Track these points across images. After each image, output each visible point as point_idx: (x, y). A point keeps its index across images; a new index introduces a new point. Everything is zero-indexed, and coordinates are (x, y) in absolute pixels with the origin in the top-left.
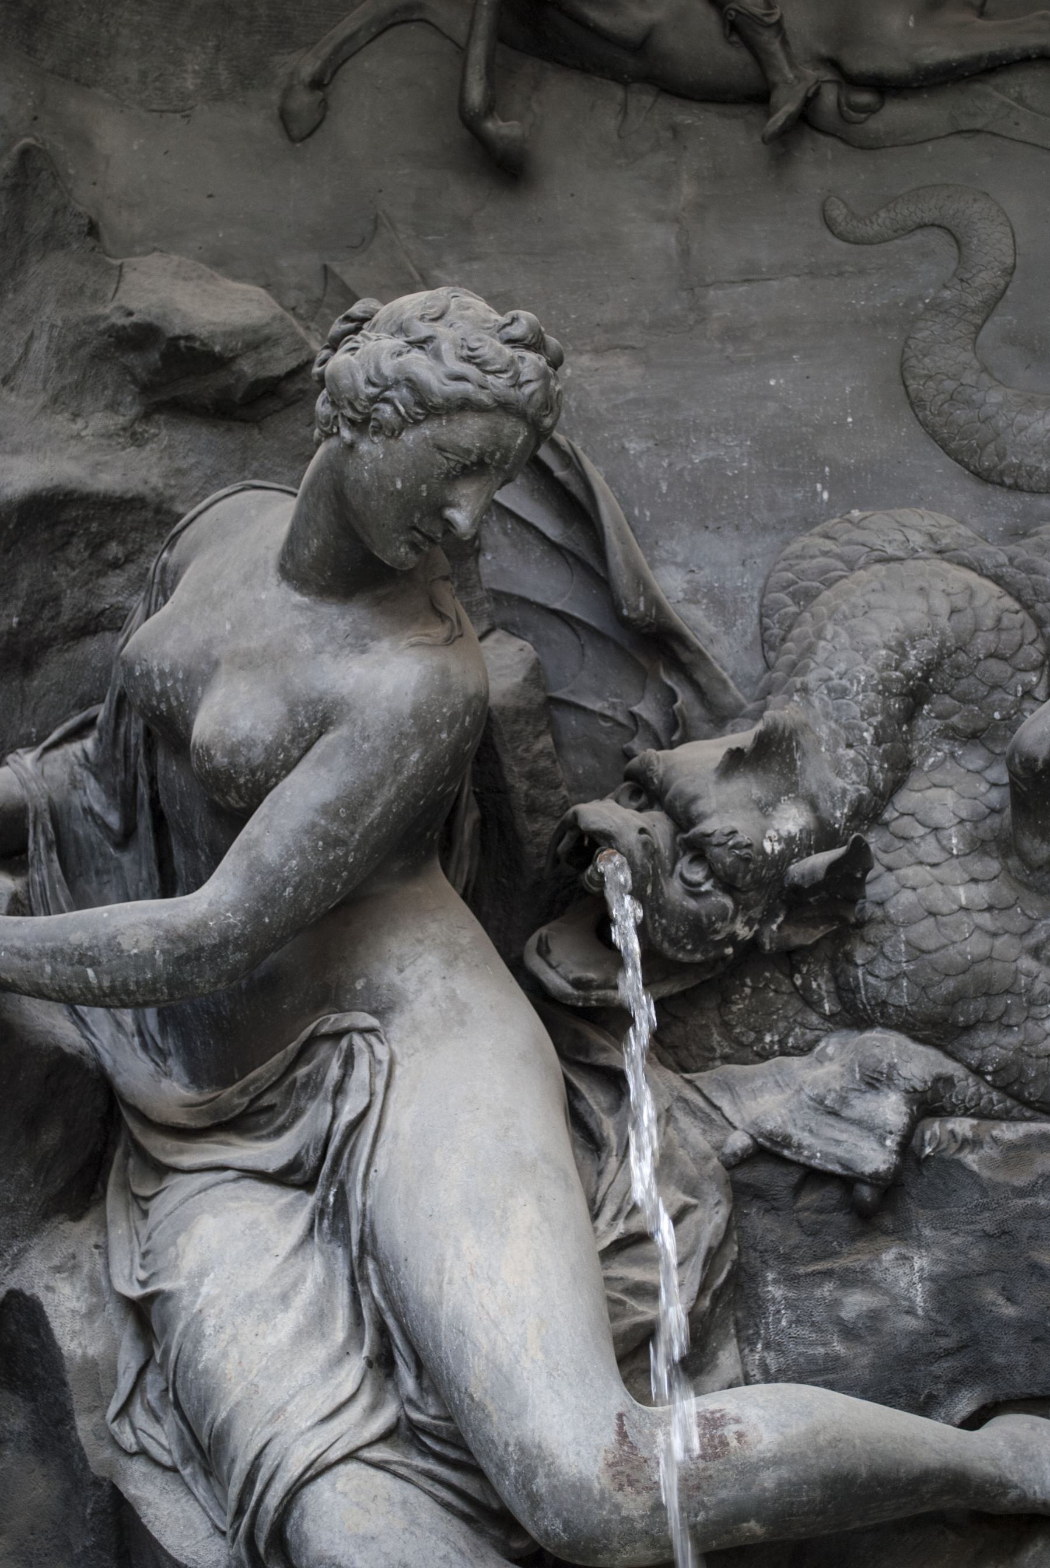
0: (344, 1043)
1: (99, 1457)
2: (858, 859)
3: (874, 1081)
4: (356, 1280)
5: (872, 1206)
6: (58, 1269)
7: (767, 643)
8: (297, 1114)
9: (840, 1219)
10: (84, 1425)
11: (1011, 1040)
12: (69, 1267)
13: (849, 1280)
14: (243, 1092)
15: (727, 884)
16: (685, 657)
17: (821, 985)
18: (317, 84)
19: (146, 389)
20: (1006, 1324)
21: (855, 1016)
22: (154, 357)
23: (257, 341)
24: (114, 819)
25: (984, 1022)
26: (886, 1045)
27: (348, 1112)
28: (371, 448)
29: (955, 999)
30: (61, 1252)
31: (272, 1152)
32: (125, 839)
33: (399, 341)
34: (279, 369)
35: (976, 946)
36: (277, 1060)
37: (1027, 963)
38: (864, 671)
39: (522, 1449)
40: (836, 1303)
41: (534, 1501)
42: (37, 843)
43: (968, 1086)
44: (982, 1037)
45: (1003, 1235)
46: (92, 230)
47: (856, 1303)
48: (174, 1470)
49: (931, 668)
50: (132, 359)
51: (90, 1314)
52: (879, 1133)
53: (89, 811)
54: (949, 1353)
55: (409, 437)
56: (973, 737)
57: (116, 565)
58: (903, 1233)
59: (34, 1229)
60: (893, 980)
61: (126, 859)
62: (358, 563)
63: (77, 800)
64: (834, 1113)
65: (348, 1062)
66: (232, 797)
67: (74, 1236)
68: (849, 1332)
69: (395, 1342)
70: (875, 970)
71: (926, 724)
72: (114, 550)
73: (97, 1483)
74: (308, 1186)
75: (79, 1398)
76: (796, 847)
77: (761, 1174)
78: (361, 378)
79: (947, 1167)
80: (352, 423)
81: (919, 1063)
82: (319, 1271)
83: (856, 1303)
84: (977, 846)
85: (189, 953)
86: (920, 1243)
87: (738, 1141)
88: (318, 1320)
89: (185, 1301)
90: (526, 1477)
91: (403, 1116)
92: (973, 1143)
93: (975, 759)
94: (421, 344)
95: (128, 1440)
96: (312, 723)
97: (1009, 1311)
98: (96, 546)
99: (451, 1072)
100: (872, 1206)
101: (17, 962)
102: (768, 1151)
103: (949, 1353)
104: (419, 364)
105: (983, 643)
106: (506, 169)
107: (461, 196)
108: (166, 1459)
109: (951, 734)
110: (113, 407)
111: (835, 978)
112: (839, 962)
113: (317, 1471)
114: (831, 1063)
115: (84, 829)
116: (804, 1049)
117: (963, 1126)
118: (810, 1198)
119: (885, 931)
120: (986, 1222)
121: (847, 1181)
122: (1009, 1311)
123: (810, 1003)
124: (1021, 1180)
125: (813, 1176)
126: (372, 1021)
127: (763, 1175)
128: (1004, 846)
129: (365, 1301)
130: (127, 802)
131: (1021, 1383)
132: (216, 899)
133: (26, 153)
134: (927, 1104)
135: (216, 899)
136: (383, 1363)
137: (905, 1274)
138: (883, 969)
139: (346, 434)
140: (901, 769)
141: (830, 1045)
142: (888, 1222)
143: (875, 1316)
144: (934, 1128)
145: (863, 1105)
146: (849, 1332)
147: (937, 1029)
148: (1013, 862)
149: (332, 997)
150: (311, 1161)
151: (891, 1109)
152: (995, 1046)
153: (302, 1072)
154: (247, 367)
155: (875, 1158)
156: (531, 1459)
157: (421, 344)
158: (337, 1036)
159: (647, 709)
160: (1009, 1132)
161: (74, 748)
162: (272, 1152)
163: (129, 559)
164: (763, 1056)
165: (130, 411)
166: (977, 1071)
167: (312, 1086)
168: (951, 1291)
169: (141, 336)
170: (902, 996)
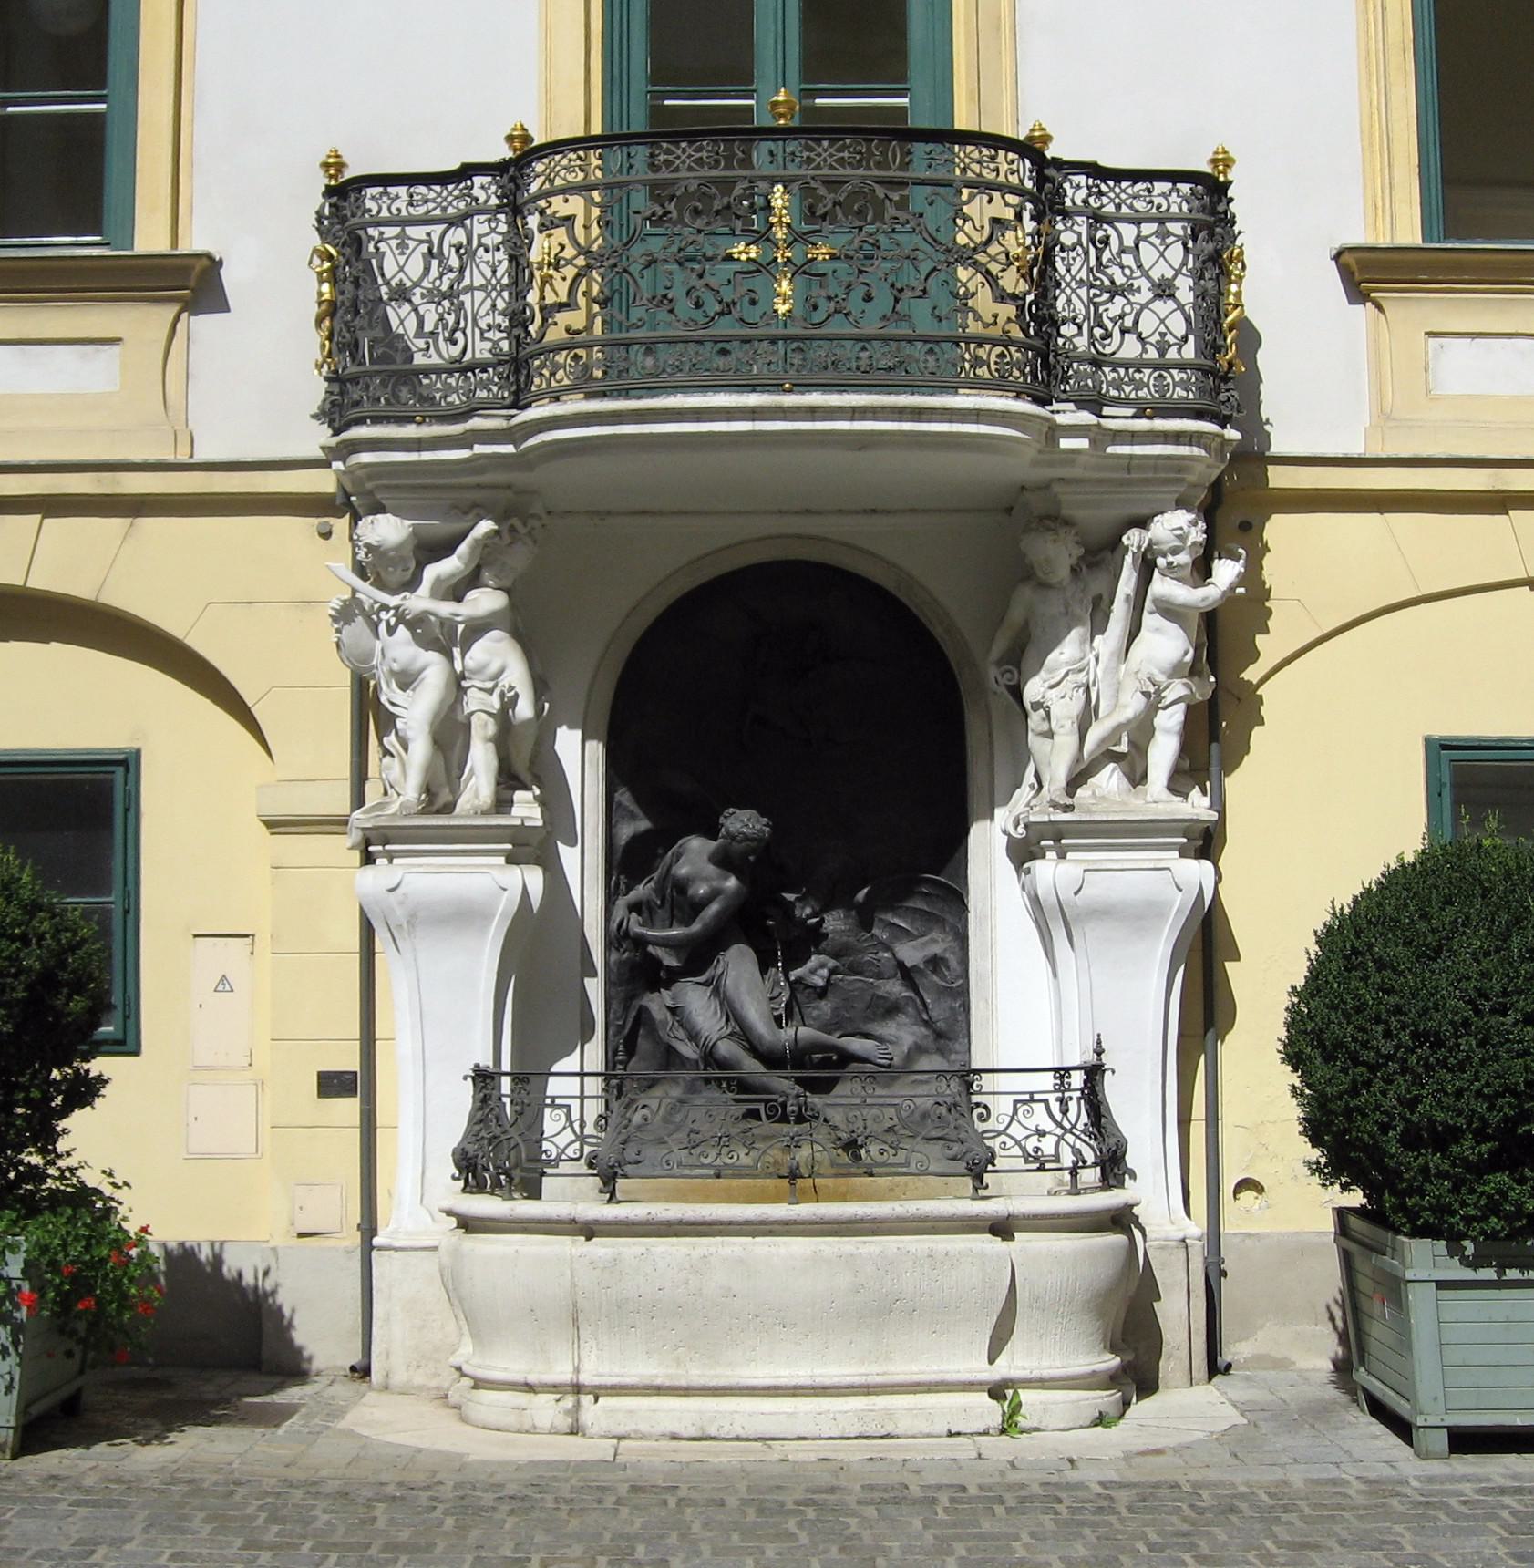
1: (666, 1039)
2: (823, 920)
3: (823, 966)
4: (721, 1004)
5: (822, 993)
26: (823, 958)
27: (719, 971)
31: (702, 979)
32: (661, 906)
62: (724, 861)
66: (697, 907)
69: (732, 1014)
76: (809, 917)
79: (835, 985)
81: (832, 963)
82: (715, 1003)
91: (732, 973)
99: (738, 965)
121: (815, 988)
125: (808, 986)
127: (796, 986)
131: (850, 1030)
132: (696, 927)
134: (833, 972)
135: (696, 927)
136: (728, 1020)
137: (826, 1007)
147: (836, 956)
151: (825, 972)
155: (821, 983)
156: (760, 1037)
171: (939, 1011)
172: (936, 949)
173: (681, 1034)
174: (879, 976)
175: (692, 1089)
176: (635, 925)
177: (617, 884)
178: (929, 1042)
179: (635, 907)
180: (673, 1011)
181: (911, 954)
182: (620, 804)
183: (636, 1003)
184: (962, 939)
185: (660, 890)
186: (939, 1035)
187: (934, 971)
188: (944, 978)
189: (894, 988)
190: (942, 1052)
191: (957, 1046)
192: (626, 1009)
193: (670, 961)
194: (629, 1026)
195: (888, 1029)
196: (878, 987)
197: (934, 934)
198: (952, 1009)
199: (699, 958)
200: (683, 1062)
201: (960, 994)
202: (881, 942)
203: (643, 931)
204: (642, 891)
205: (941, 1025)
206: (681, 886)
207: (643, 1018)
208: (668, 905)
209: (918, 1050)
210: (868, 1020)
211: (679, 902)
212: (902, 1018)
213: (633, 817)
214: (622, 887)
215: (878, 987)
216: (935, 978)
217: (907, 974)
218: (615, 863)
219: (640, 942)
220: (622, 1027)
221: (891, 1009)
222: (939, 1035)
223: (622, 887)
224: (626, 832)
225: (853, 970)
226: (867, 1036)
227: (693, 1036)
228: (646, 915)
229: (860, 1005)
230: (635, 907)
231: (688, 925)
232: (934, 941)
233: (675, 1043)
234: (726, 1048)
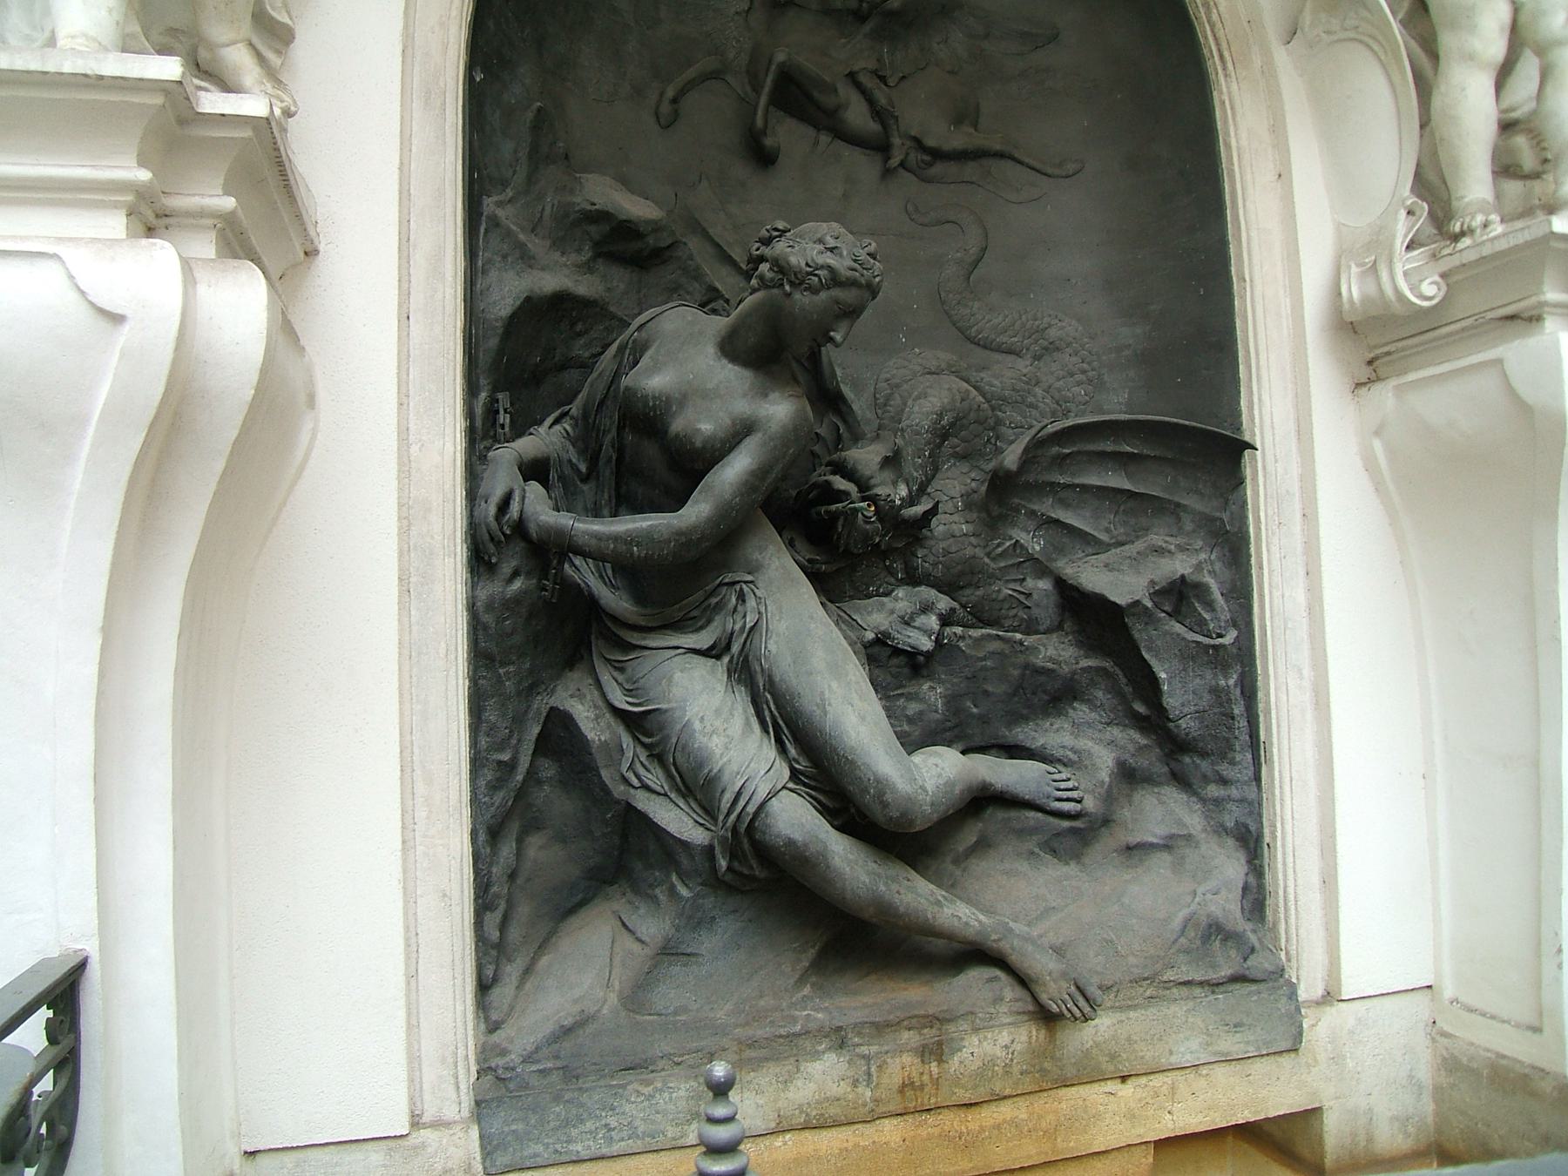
0: (738, 587)
1: (618, 790)
3: (926, 609)
6: (572, 696)
7: (880, 405)
8: (709, 622)
9: (906, 670)
10: (605, 774)
11: (980, 592)
12: (579, 695)
13: (910, 697)
14: (680, 609)
15: (880, 520)
16: (844, 409)
17: (897, 565)
18: (674, 101)
19: (596, 244)
20: (972, 716)
21: (913, 579)
22: (606, 228)
23: (657, 227)
24: (583, 468)
25: (969, 585)
28: (802, 299)
29: (962, 574)
30: (572, 687)
31: (704, 639)
32: (585, 479)
33: (821, 247)
34: (663, 244)
35: (969, 552)
36: (699, 595)
37: (986, 560)
38: (926, 424)
39: (878, 781)
40: (905, 708)
41: (885, 805)
42: (553, 475)
43: (960, 612)
44: (968, 592)
45: (972, 678)
46: (567, 157)
47: (913, 708)
48: (666, 795)
49: (952, 425)
50: (593, 229)
51: (597, 717)
52: (928, 633)
53: (570, 461)
54: (950, 729)
55: (823, 295)
56: (964, 457)
57: (580, 334)
58: (930, 677)
59: (559, 676)
60: (935, 565)
61: (585, 488)
63: (565, 457)
64: (908, 624)
65: (742, 597)
67: (577, 678)
68: (910, 720)
70: (924, 559)
71: (947, 447)
72: (579, 327)
73: (618, 802)
74: (718, 657)
75: (600, 761)
77: (876, 650)
78: (803, 264)
80: (792, 283)
81: (944, 603)
83: (913, 708)
84: (968, 506)
85: (685, 539)
86: (940, 682)
87: (870, 636)
88: (748, 723)
89: (677, 714)
90: (880, 795)
92: (962, 638)
93: (964, 467)
94: (831, 250)
95: (635, 782)
96: (743, 430)
97: (975, 710)
98: (573, 325)
100: (916, 664)
101: (594, 542)
102: (881, 640)
103: (950, 729)
104: (829, 259)
105: (972, 415)
106: (763, 157)
107: (740, 170)
108: (659, 789)
109: (956, 456)
110: (579, 251)
111: (906, 563)
112: (907, 554)
113: (773, 794)
114: (903, 599)
115: (567, 471)
116: (887, 594)
117: (959, 630)
118: (895, 661)
119: (932, 543)
120: (967, 672)
122: (975, 710)
123: (893, 574)
124: (981, 655)
125: (897, 652)
126: (750, 578)
128: (983, 507)
129: (767, 713)
130: (593, 461)
133: (539, 110)
136: (779, 742)
137: (932, 694)
138: (931, 559)
139: (787, 288)
140: (936, 470)
141: (900, 592)
142: (925, 672)
143: (921, 713)
144: (948, 630)
145: (921, 620)
146: (910, 720)
148: (984, 515)
149: (726, 566)
150: (723, 644)
151: (933, 622)
152: (972, 595)
153: (714, 600)
154: (651, 240)
155: (926, 644)
156: (882, 785)
157: (831, 250)
158: (734, 583)
159: (823, 431)
160: (976, 633)
161: (558, 427)
162: (704, 639)
163: (586, 332)
164: (869, 596)
165: (587, 254)
166: (964, 606)
167: (719, 607)
168: (952, 700)
169: (602, 216)
170: (939, 571)
171: (1182, 695)
172: (1180, 566)
173: (656, 778)
174: (1030, 628)
175: (695, 921)
176: (538, 506)
177: (491, 412)
178: (1151, 761)
179: (535, 470)
180: (635, 722)
181: (1118, 579)
182: (495, 223)
183: (542, 704)
184: (1234, 546)
185: (586, 437)
186: (1174, 746)
187: (1175, 614)
188: (1200, 626)
189: (1057, 652)
190: (1181, 780)
191: (1225, 769)
192: (519, 721)
193: (615, 600)
194: (524, 762)
195: (1054, 734)
196: (1033, 649)
197: (1157, 539)
198: (1215, 691)
199: (683, 588)
200: (667, 848)
201: (1236, 663)
202: (1031, 558)
203: (565, 520)
204: (545, 439)
205: (1187, 725)
206: (646, 419)
207: (559, 737)
208: (607, 472)
209: (1129, 776)
210: (1017, 718)
211: (643, 455)
212: (1081, 712)
213: (526, 259)
214: (504, 418)
215: (1033, 649)
216: (1178, 628)
217: (1091, 617)
218: (484, 359)
219: (546, 552)
220: (510, 766)
221: (1058, 695)
222: (1174, 746)
223: (504, 418)
224: (509, 290)
225: (980, 616)
226: (1014, 751)
227: (696, 786)
228: (558, 491)
229: (997, 688)
230: (535, 470)
231: (677, 501)
232: (1159, 551)
233: (643, 801)
234: (796, 818)
